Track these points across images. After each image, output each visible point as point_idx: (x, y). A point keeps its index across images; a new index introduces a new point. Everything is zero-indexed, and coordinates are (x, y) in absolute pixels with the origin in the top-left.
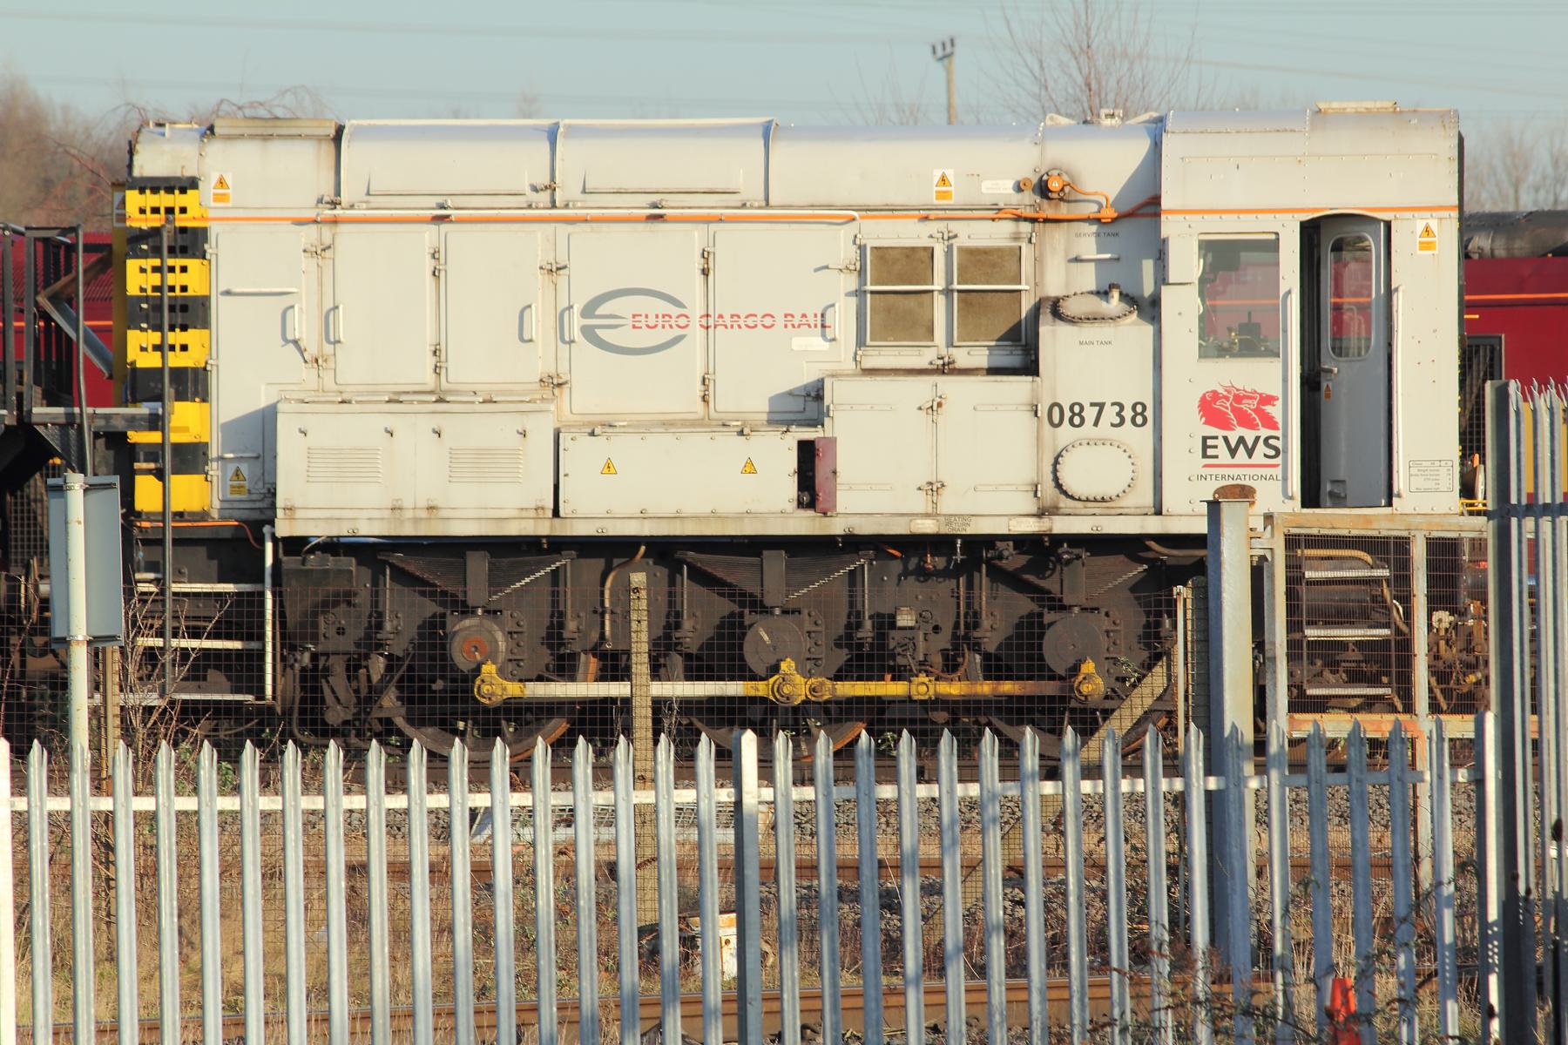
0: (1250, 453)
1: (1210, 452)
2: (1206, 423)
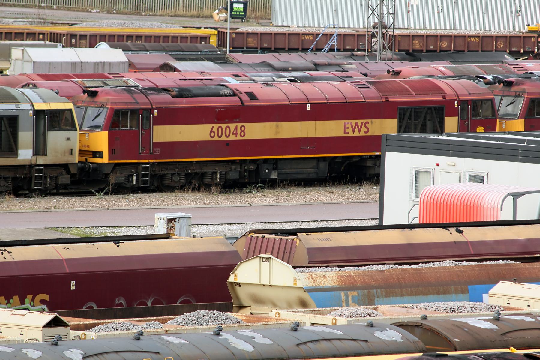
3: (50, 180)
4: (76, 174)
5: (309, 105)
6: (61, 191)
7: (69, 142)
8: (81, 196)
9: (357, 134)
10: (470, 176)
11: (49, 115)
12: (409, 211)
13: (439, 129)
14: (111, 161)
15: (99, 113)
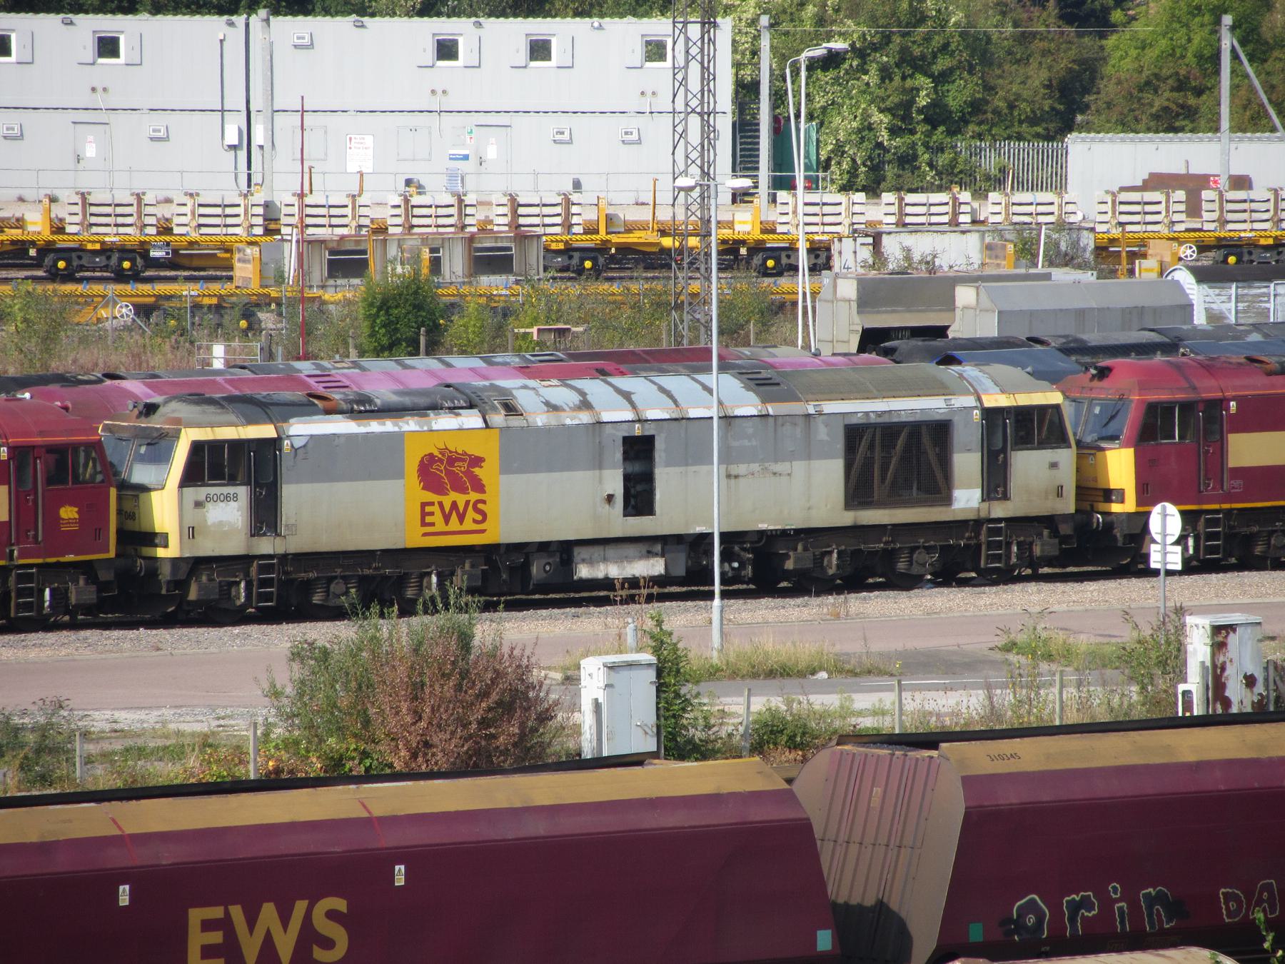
0: (461, 518)
1: (428, 519)
2: (424, 488)
4: (1069, 537)
6: (1042, 571)
7: (1054, 471)
11: (1013, 417)
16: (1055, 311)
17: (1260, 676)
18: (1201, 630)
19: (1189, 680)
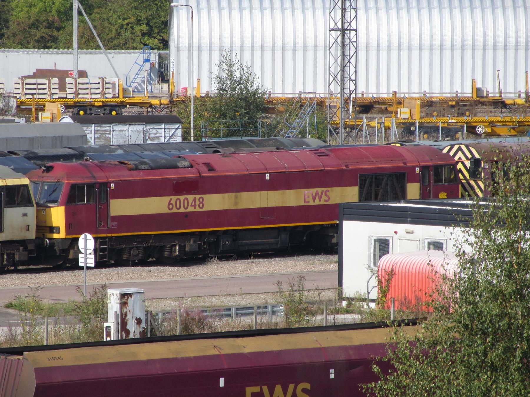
3: (7, 257)
5: (268, 175)
6: (20, 268)
7: (25, 218)
8: (39, 273)
9: (317, 202)
10: (429, 243)
12: (368, 279)
13: (401, 195)
14: (68, 237)
15: (55, 188)
16: (19, 138)
17: (143, 319)
18: (115, 296)
19: (109, 320)
